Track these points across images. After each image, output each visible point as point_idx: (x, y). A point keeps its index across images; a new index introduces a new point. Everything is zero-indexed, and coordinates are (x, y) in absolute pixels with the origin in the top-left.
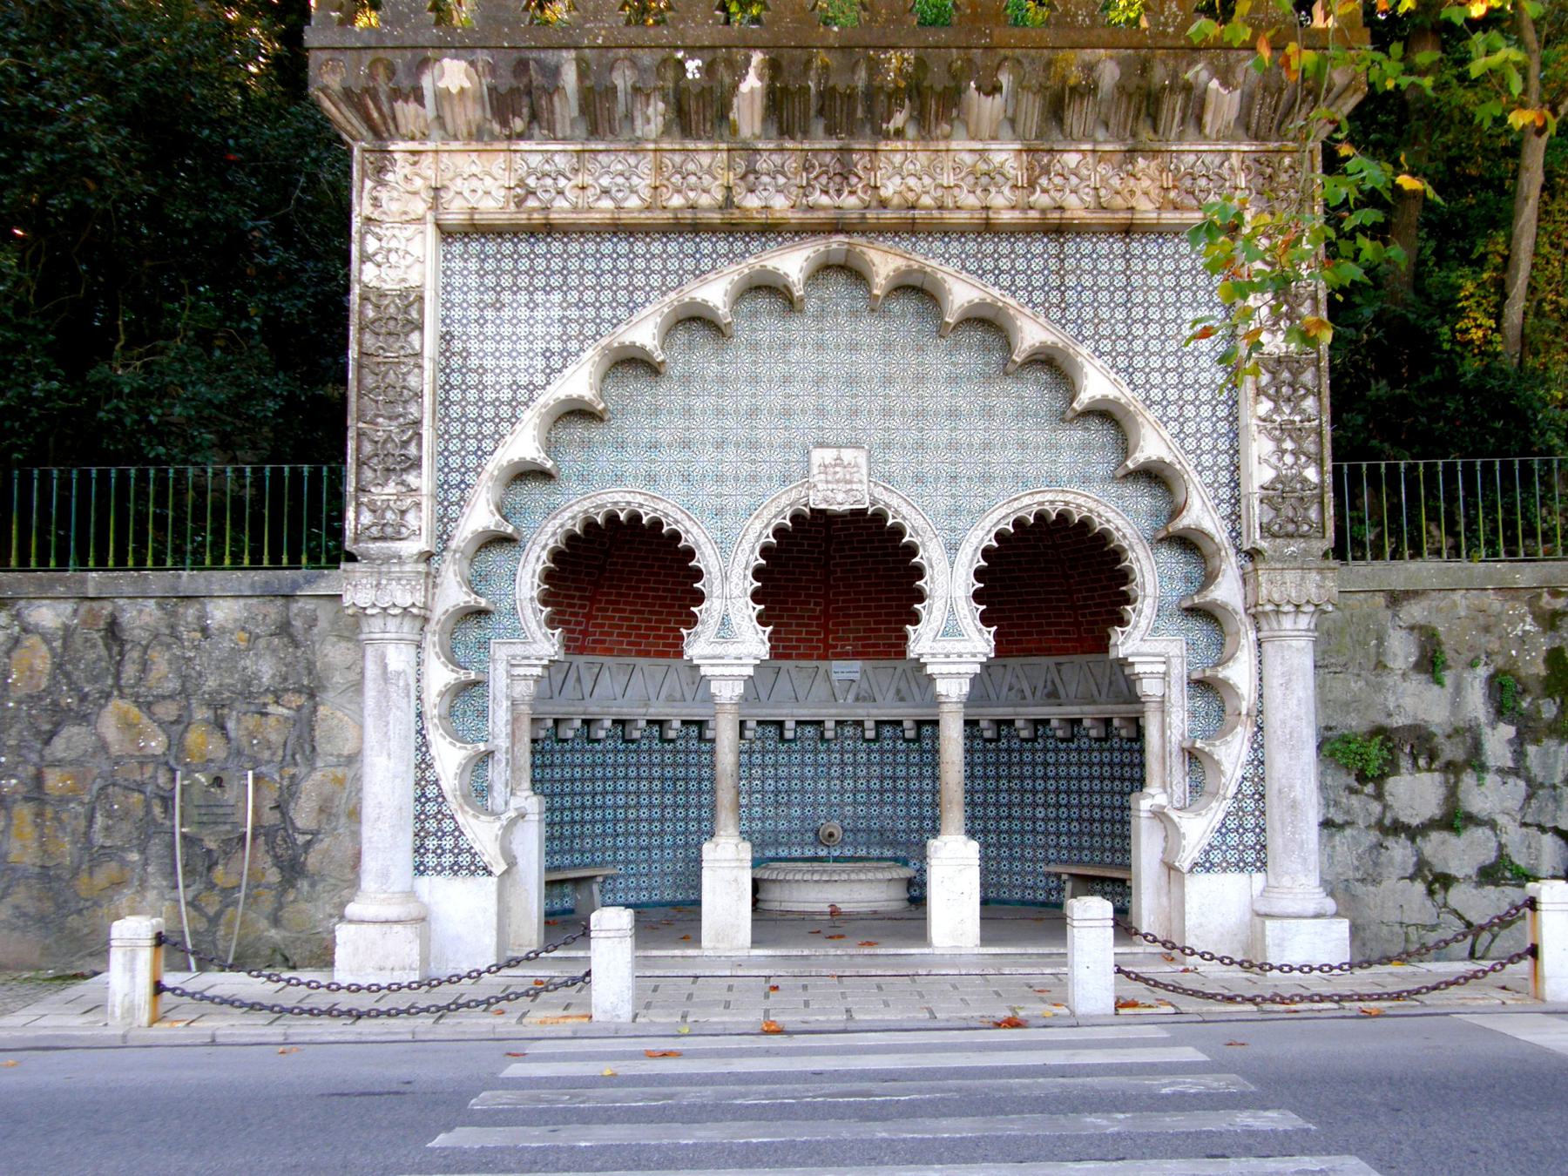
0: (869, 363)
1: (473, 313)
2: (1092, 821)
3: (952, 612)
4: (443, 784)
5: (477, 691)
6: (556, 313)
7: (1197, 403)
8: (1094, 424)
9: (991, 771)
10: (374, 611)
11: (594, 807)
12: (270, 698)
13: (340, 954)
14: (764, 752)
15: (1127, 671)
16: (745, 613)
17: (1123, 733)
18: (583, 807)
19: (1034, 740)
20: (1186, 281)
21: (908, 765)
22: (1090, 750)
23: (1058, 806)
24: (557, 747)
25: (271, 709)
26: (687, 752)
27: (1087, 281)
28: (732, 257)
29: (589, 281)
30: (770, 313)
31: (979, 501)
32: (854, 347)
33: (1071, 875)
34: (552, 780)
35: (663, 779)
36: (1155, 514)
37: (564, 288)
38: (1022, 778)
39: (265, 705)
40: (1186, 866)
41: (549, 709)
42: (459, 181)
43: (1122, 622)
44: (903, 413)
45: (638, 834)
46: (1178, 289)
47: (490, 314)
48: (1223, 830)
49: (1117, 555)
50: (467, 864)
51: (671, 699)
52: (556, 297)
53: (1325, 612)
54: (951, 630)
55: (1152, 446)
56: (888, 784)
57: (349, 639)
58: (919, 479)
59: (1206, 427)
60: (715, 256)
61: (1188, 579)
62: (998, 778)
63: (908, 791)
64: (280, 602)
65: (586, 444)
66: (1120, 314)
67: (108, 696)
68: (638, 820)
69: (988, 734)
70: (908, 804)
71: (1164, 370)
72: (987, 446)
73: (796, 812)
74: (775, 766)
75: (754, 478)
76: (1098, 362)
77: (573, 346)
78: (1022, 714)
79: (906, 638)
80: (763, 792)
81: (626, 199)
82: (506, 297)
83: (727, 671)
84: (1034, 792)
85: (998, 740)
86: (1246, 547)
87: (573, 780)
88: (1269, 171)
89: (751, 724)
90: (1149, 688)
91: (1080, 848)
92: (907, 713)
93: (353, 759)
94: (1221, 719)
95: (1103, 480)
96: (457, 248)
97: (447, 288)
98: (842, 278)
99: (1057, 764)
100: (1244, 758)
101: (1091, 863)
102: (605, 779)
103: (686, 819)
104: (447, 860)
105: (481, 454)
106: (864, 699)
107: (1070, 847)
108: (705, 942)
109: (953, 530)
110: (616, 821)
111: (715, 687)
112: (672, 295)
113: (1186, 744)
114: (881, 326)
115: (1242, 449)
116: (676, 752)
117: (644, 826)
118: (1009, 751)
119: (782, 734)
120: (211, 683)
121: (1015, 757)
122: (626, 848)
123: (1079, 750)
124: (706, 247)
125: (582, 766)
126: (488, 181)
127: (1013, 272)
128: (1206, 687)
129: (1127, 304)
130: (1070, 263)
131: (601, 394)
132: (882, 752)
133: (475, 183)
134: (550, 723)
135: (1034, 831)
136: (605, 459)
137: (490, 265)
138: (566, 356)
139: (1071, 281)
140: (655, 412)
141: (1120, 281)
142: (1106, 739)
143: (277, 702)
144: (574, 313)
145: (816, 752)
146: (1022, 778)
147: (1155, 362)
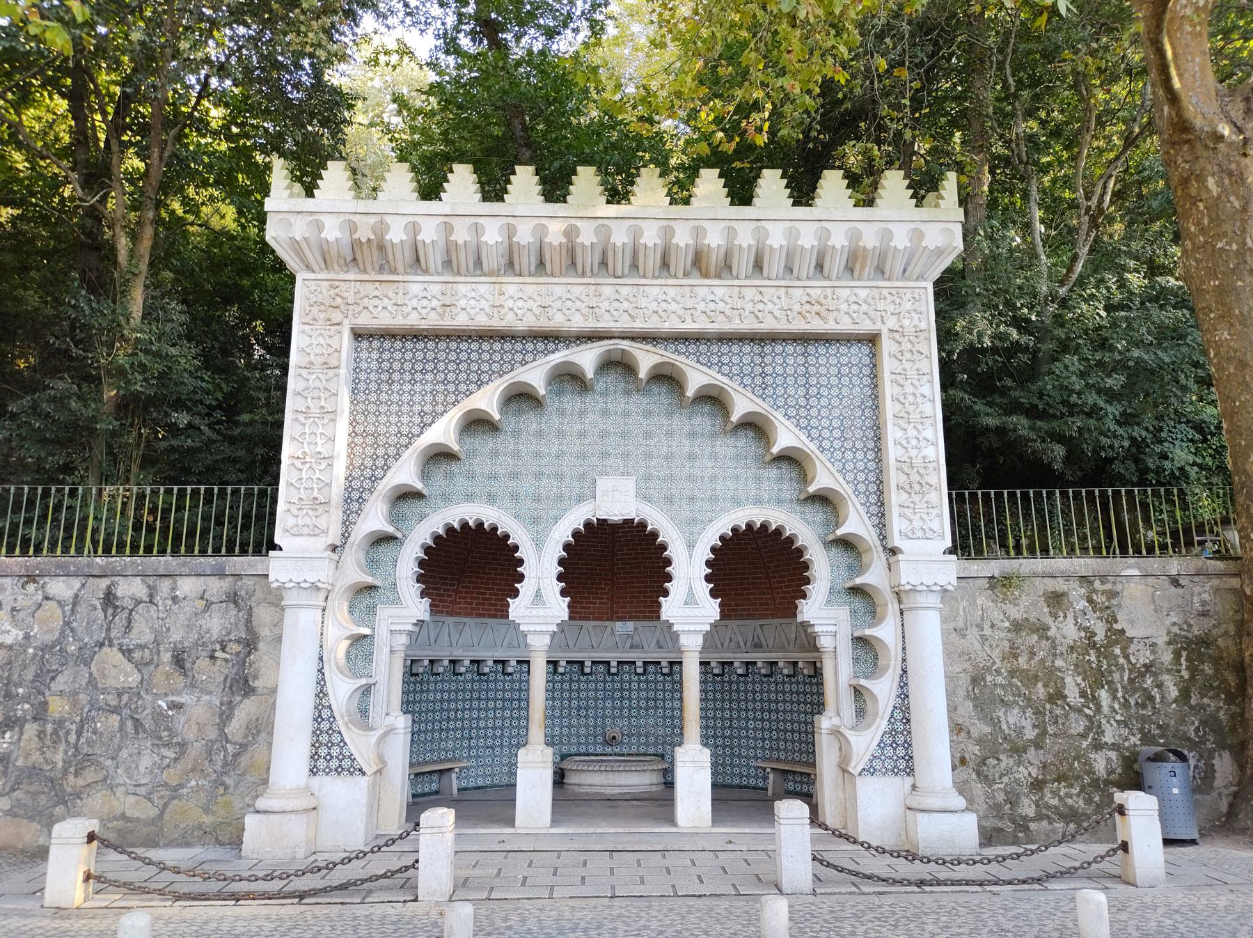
0: (637, 424)
1: (373, 386)
2: (786, 731)
3: (690, 588)
4: (334, 707)
5: (364, 642)
6: (429, 387)
7: (854, 449)
8: (784, 465)
9: (718, 696)
10: (291, 585)
11: (456, 719)
12: (218, 647)
13: (247, 837)
14: (571, 681)
15: (809, 630)
16: (554, 587)
17: (806, 672)
18: (449, 719)
19: (746, 675)
20: (845, 370)
21: (664, 691)
22: (783, 683)
23: (762, 720)
24: (432, 679)
25: (217, 654)
26: (520, 681)
27: (779, 370)
28: (546, 353)
29: (452, 366)
30: (572, 392)
31: (709, 514)
32: (626, 414)
33: (772, 769)
34: (428, 701)
35: (504, 700)
36: (827, 524)
37: (435, 371)
38: (739, 700)
39: (214, 651)
40: (856, 771)
41: (426, 653)
42: (366, 300)
43: (804, 596)
44: (659, 456)
45: (486, 737)
46: (839, 375)
47: (384, 387)
48: (881, 745)
49: (800, 552)
50: (348, 767)
51: (510, 646)
52: (429, 377)
53: (946, 591)
54: (690, 600)
55: (823, 479)
56: (651, 703)
57: (277, 606)
58: (669, 500)
59: (860, 465)
60: (535, 353)
61: (850, 568)
62: (723, 700)
63: (665, 709)
64: (230, 579)
65: (449, 476)
66: (801, 391)
67: (101, 645)
68: (486, 728)
69: (716, 671)
70: (664, 718)
71: (831, 428)
72: (713, 478)
73: (591, 722)
74: (578, 691)
75: (560, 498)
76: (787, 423)
77: (440, 408)
78: (738, 658)
79: (659, 606)
80: (570, 709)
81: (476, 314)
82: (396, 376)
83: (538, 628)
84: (747, 710)
85: (723, 675)
86: (889, 546)
87: (442, 701)
88: (898, 300)
89: (563, 663)
90: (825, 642)
91: (778, 750)
92: (664, 657)
93: (274, 691)
94: (875, 665)
95: (791, 501)
96: (365, 344)
97: (357, 370)
98: (619, 369)
99: (761, 692)
100: (895, 691)
101: (785, 761)
102: (464, 700)
103: (518, 727)
104: (334, 764)
105: (374, 479)
106: (637, 647)
107: (771, 749)
108: (517, 823)
109: (692, 533)
110: (471, 728)
111: (530, 639)
112: (507, 377)
113: (854, 682)
114: (644, 401)
115: (885, 480)
116: (512, 682)
117: (490, 733)
118: (730, 682)
119: (582, 670)
120: (176, 636)
121: (734, 687)
122: (477, 748)
123: (776, 683)
124: (530, 346)
125: (449, 691)
126: (386, 300)
127: (731, 364)
128: (863, 643)
129: (807, 385)
130: (768, 359)
131: (460, 441)
132: (647, 682)
133: (376, 302)
134: (426, 663)
135: (747, 737)
136: (461, 484)
137: (386, 355)
138: (436, 416)
139: (769, 370)
140: (495, 454)
141: (801, 370)
142: (793, 676)
143: (223, 649)
144: (441, 387)
145: (605, 682)
146: (739, 700)
147: (825, 423)
